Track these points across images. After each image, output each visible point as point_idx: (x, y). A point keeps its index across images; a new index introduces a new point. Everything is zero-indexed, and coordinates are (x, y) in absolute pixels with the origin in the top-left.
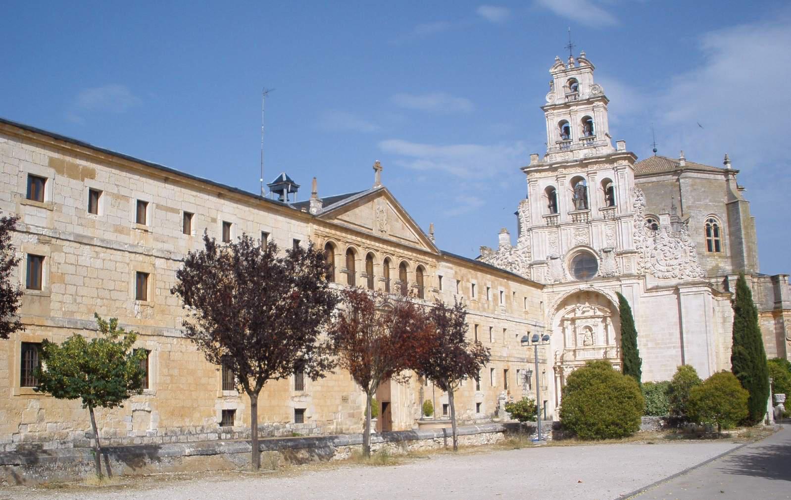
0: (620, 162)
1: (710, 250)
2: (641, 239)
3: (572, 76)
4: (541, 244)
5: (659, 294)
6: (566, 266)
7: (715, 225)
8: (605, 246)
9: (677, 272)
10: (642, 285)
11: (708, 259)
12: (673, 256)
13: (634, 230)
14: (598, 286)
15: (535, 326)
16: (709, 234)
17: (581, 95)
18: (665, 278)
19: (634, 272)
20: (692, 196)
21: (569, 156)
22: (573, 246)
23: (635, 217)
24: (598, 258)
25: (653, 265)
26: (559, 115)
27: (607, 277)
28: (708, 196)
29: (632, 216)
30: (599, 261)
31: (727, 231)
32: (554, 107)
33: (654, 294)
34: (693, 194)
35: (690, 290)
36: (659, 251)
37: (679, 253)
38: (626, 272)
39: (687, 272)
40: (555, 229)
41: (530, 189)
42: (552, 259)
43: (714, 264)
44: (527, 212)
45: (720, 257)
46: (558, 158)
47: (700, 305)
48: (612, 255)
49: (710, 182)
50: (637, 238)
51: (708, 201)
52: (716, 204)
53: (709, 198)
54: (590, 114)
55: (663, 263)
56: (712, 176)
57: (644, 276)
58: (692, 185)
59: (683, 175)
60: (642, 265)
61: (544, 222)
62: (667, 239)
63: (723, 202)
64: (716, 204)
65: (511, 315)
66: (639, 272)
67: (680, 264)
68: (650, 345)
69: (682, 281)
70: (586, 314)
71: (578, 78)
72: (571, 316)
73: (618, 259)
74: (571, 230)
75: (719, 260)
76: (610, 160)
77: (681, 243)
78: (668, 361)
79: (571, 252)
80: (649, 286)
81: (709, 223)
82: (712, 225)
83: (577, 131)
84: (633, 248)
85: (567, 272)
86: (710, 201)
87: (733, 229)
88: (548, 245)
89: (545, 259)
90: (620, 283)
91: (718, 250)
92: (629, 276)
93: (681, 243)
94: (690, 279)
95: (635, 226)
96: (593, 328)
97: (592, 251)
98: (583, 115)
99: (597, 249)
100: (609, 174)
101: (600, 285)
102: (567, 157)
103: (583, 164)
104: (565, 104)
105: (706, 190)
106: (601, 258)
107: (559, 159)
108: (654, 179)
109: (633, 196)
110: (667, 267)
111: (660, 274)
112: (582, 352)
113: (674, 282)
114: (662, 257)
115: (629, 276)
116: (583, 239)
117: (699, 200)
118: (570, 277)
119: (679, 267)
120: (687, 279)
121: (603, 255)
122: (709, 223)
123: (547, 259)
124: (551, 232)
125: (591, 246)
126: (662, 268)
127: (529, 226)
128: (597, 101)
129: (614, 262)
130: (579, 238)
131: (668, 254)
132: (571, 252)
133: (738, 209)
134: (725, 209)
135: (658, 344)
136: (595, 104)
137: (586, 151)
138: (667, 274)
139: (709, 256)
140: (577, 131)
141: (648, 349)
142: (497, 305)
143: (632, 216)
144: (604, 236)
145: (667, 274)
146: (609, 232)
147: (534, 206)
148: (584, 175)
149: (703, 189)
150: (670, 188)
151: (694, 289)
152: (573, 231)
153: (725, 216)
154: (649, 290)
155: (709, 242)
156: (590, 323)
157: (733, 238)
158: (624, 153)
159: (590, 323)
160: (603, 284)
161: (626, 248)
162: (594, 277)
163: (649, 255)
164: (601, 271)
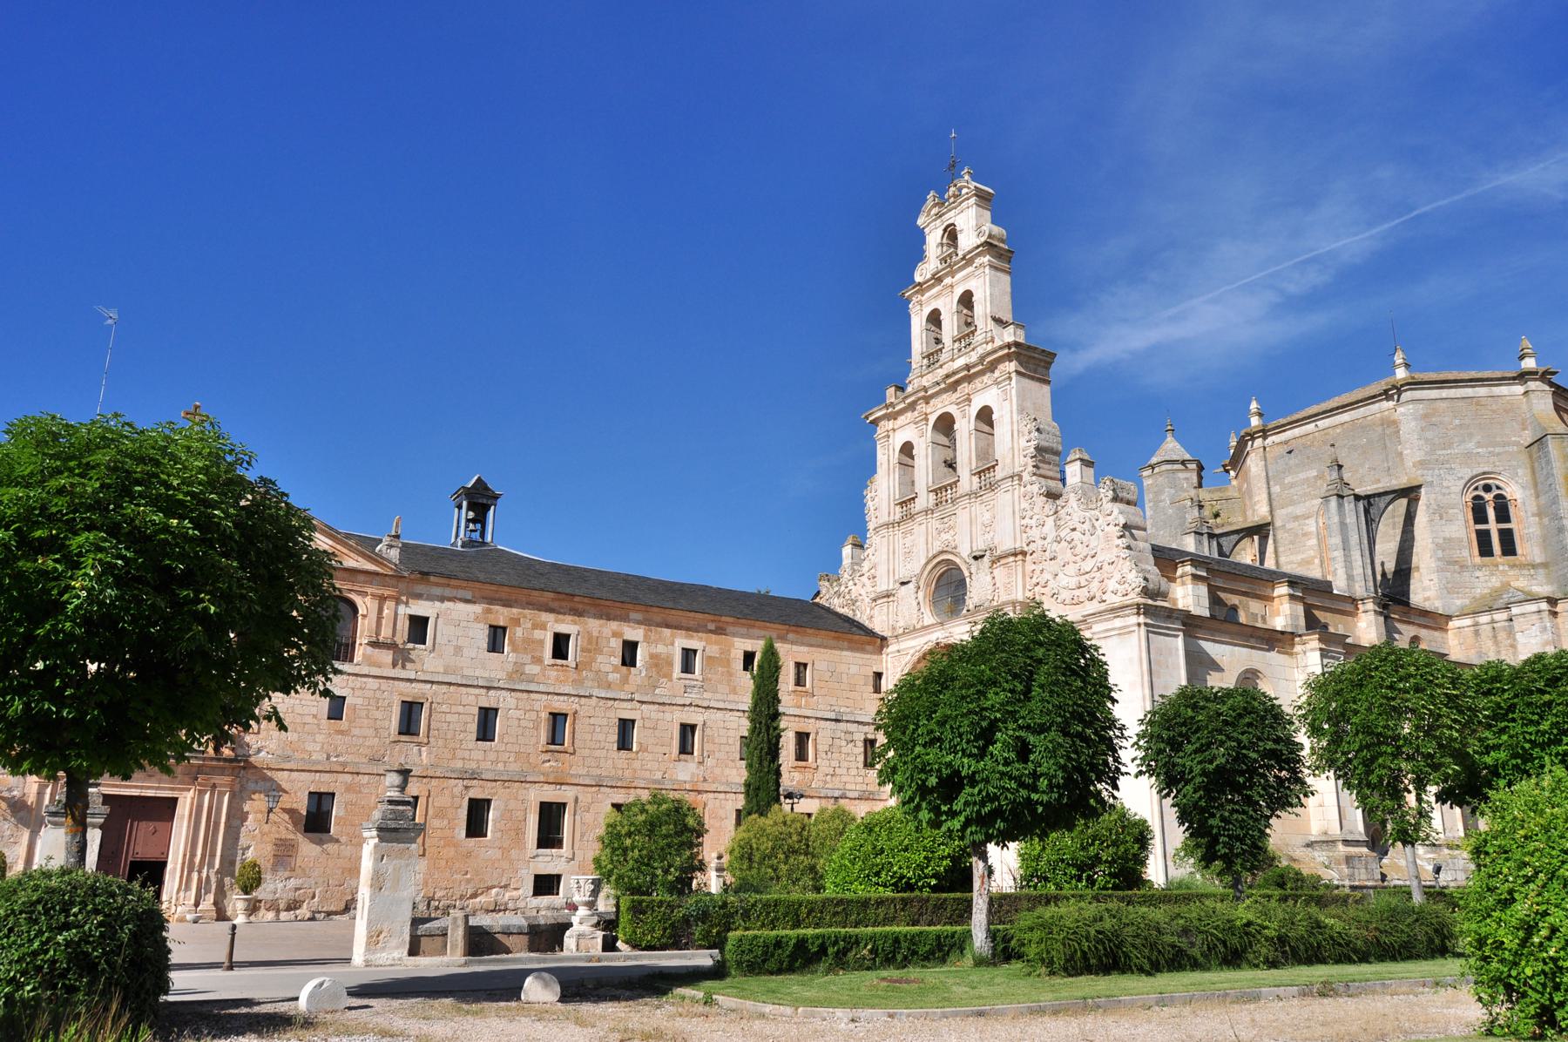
0: (1001, 367)
1: (1485, 549)
2: (1033, 522)
6: (921, 594)
7: (1499, 497)
8: (980, 545)
11: (1478, 574)
12: (1085, 551)
15: (837, 721)
16: (1479, 514)
20: (1427, 440)
24: (966, 574)
28: (1471, 435)
31: (1532, 506)
34: (1429, 435)
35: (1108, 625)
42: (903, 584)
43: (1495, 582)
45: (1513, 566)
49: (1477, 404)
51: (1471, 445)
52: (1497, 450)
53: (1478, 438)
56: (1482, 391)
58: (1425, 416)
59: (1406, 396)
61: (898, 513)
63: (1517, 444)
64: (1497, 450)
65: (731, 697)
67: (1100, 569)
74: (934, 523)
75: (1511, 573)
81: (1482, 493)
82: (1488, 497)
83: (950, 327)
84: (1020, 544)
86: (1479, 445)
87: (1543, 500)
91: (1509, 547)
98: (959, 291)
105: (1467, 421)
108: (1346, 417)
111: (1065, 595)
117: (1450, 446)
118: (929, 619)
122: (1482, 493)
128: (978, 255)
129: (989, 578)
130: (944, 536)
131: (1080, 549)
133: (1547, 454)
134: (1524, 457)
139: (1480, 568)
140: (950, 327)
142: (669, 676)
145: (1077, 592)
148: (952, 409)
149: (1457, 422)
150: (1380, 429)
151: (1118, 623)
153: (1523, 473)
155: (1483, 540)
157: (1546, 520)
161: (1007, 545)
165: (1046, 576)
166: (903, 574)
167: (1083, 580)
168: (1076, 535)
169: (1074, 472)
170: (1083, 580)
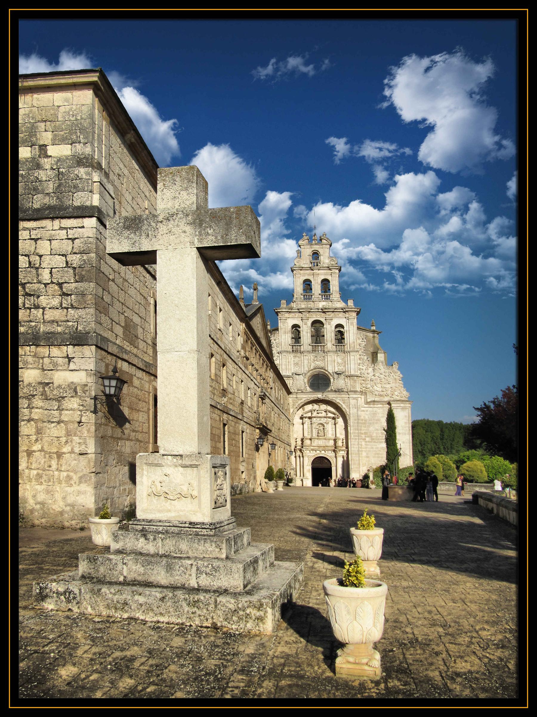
2: (364, 368)
3: (316, 249)
4: (287, 363)
5: (376, 406)
6: (306, 380)
8: (336, 370)
9: (389, 392)
10: (363, 400)
13: (359, 362)
14: (331, 396)
17: (321, 263)
18: (381, 396)
19: (359, 390)
21: (311, 305)
22: (312, 368)
23: (360, 353)
24: (331, 378)
25: (372, 387)
26: (304, 275)
27: (339, 391)
29: (358, 351)
30: (332, 380)
32: (302, 269)
33: (372, 406)
36: (376, 377)
37: (391, 380)
38: (352, 389)
39: (396, 393)
40: (299, 354)
41: (280, 325)
44: (277, 341)
46: (303, 305)
47: (406, 416)
48: (342, 376)
50: (361, 367)
54: (329, 278)
55: (379, 386)
57: (366, 393)
60: (364, 385)
62: (383, 370)
66: (361, 390)
68: (367, 439)
69: (392, 399)
70: (320, 415)
71: (321, 251)
72: (309, 415)
73: (346, 380)
74: (311, 356)
76: (344, 311)
77: (393, 374)
78: (380, 451)
79: (311, 372)
80: (369, 400)
83: (317, 288)
84: (358, 373)
85: (307, 385)
88: (292, 365)
89: (291, 374)
90: (348, 396)
92: (355, 392)
93: (393, 374)
94: (398, 398)
95: (360, 359)
96: (325, 425)
97: (327, 372)
98: (323, 277)
99: (331, 372)
100: (343, 322)
101: (333, 396)
102: (309, 306)
103: (324, 311)
104: (310, 268)
106: (334, 378)
107: (303, 306)
109: (359, 339)
110: (381, 389)
111: (377, 393)
112: (316, 441)
113: (386, 399)
114: (379, 381)
115: (355, 392)
116: (320, 363)
118: (309, 389)
119: (390, 389)
120: (395, 397)
121: (336, 376)
123: (293, 374)
124: (296, 357)
125: (326, 369)
126: (378, 389)
127: (279, 350)
130: (317, 363)
131: (383, 380)
132: (311, 372)
135: (374, 439)
136: (334, 271)
137: (324, 303)
138: (382, 393)
140: (317, 288)
141: (366, 442)
143: (358, 351)
144: (336, 364)
146: (340, 361)
147: (283, 337)
148: (323, 320)
151: (402, 405)
152: (312, 358)
154: (367, 403)
156: (323, 421)
158: (352, 308)
159: (323, 421)
160: (335, 396)
161: (353, 373)
162: (327, 390)
163: (369, 379)
164: (333, 386)
165: (369, 386)
166: (297, 370)
167: (384, 390)
168: (382, 376)
169: (381, 357)
170: (384, 390)
